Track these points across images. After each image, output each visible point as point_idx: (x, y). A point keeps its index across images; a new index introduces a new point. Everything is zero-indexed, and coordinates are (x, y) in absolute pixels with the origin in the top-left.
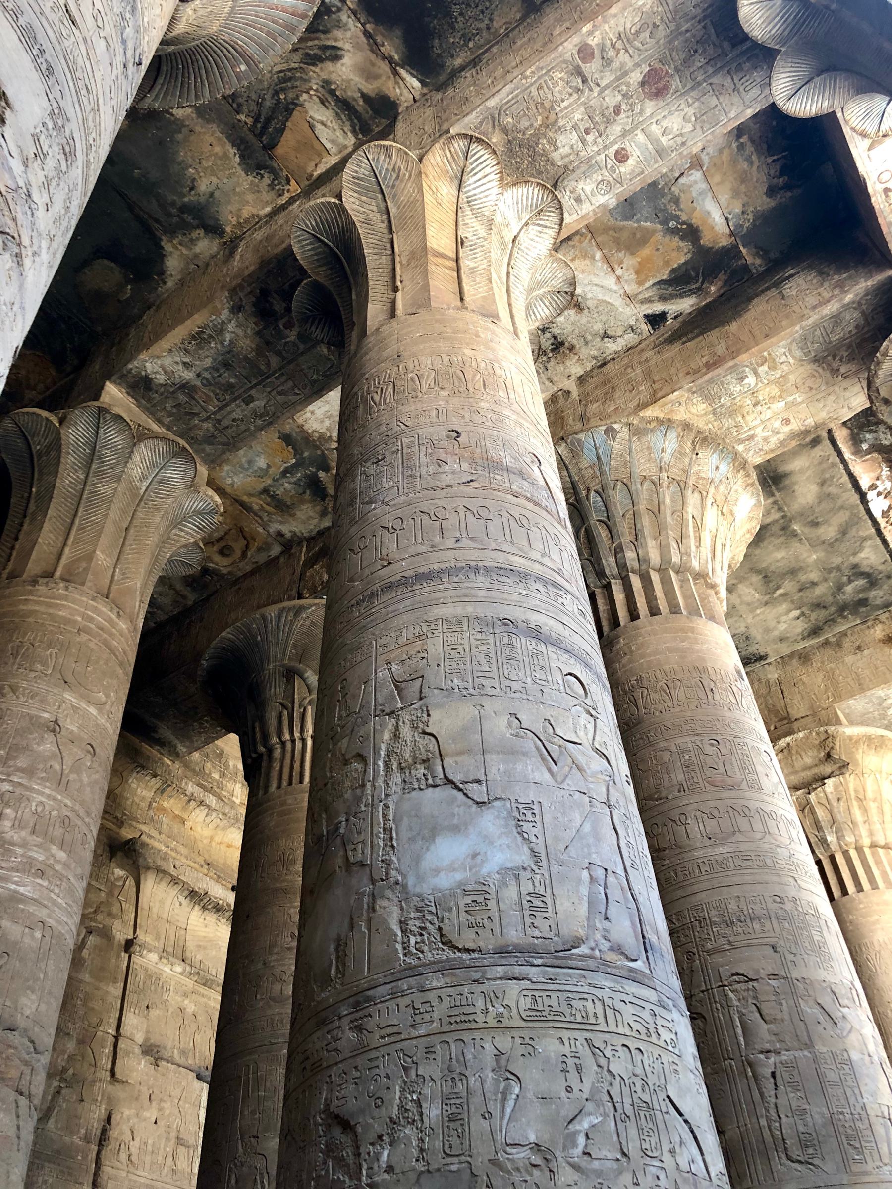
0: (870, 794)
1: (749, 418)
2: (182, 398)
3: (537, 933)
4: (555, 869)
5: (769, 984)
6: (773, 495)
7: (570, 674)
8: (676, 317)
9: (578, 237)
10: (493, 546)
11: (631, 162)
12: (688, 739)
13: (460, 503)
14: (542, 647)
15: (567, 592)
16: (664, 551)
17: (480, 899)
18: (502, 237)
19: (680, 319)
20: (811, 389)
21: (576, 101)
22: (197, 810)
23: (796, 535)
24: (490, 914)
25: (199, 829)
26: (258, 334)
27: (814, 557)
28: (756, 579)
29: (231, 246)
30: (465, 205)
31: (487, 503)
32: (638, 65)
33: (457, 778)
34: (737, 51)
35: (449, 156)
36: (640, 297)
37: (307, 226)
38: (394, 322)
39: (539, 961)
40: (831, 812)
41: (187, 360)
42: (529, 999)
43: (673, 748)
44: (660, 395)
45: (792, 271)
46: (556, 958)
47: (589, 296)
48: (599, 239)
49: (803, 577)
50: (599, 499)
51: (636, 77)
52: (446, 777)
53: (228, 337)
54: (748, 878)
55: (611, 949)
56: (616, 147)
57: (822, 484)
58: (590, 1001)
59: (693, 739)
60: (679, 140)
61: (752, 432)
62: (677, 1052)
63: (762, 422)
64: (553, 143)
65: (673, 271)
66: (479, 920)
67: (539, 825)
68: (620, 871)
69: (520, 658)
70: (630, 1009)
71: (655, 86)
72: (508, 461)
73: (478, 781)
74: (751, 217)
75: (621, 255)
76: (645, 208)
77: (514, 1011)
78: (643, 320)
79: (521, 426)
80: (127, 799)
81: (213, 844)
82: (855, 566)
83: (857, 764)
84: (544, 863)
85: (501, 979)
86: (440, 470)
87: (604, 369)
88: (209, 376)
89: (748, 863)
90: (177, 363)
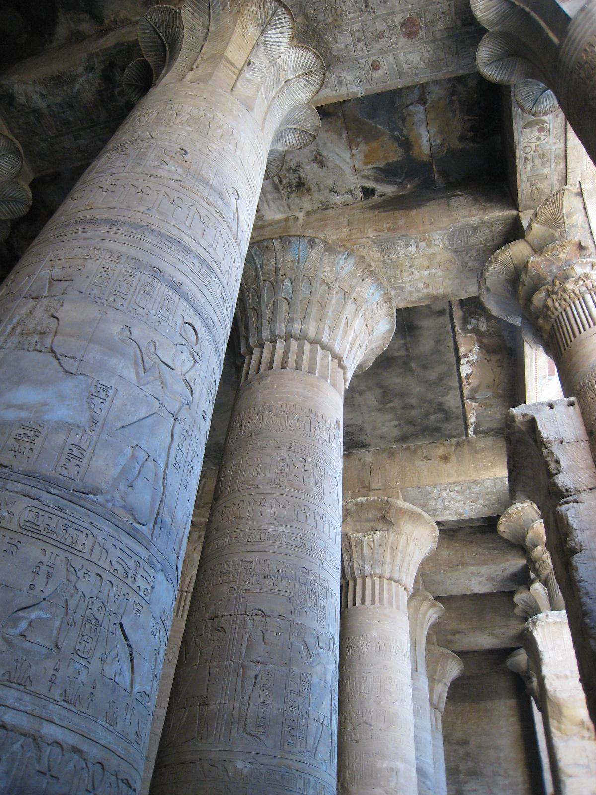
0: (400, 547)
1: (405, 274)
2: (32, 118)
3: (65, 473)
4: (104, 436)
5: (276, 621)
6: (405, 338)
7: (190, 324)
8: (381, 196)
10: (174, 222)
11: (380, 71)
12: (286, 453)
13: (163, 190)
14: (176, 297)
15: (217, 277)
16: (319, 331)
17: (31, 434)
18: (279, 75)
19: (383, 198)
20: (447, 269)
21: (358, 17)
23: (412, 371)
24: (33, 446)
26: (99, 92)
27: (418, 389)
28: (379, 391)
29: (103, 33)
30: (261, 45)
31: (184, 198)
32: (403, 12)
33: (58, 351)
35: (262, 9)
36: (363, 173)
37: (152, 21)
38: (178, 84)
39: (56, 492)
40: (373, 552)
41: (44, 93)
42: (33, 514)
43: (275, 455)
44: (354, 237)
45: (459, 193)
46: (72, 495)
47: (330, 159)
49: (407, 400)
50: (290, 284)
51: (400, 18)
52: (51, 348)
53: (78, 86)
54: (291, 552)
55: (124, 507)
56: (374, 58)
57: (438, 342)
58: (85, 535)
59: (290, 453)
60: (415, 71)
61: (404, 285)
62: (147, 598)
63: (412, 280)
64: (335, 38)
65: (388, 164)
66: (22, 447)
67: (107, 404)
68: (162, 462)
69: (155, 296)
70: (119, 553)
72: (214, 182)
73: (74, 358)
74: (445, 149)
77: (16, 518)
78: (359, 190)
79: (236, 171)
82: (440, 404)
84: (98, 429)
85: (17, 493)
86: (161, 167)
87: (326, 212)
88: (55, 110)
89: (295, 542)
90: (36, 92)
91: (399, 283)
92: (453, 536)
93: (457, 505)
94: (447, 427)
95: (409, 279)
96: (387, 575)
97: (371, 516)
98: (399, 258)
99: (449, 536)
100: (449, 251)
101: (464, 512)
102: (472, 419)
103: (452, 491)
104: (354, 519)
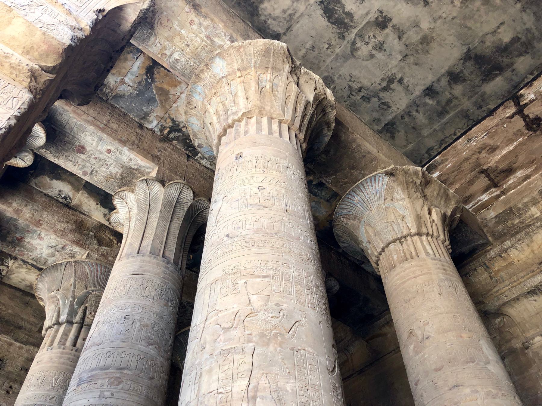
1: (197, 45)
9: (171, 116)
11: (109, 148)
20: (168, 20)
22: (510, 253)
25: (522, 256)
32: (79, 157)
34: (56, 128)
48: (168, 108)
51: (82, 156)
56: (107, 154)
60: (93, 135)
61: (205, 38)
63: (197, 36)
64: (116, 174)
71: (82, 150)
75: (171, 96)
76: (148, 95)
80: (479, 288)
81: (536, 252)
91: (206, 42)
95: (198, 38)
98: (189, 59)
100: (156, 32)
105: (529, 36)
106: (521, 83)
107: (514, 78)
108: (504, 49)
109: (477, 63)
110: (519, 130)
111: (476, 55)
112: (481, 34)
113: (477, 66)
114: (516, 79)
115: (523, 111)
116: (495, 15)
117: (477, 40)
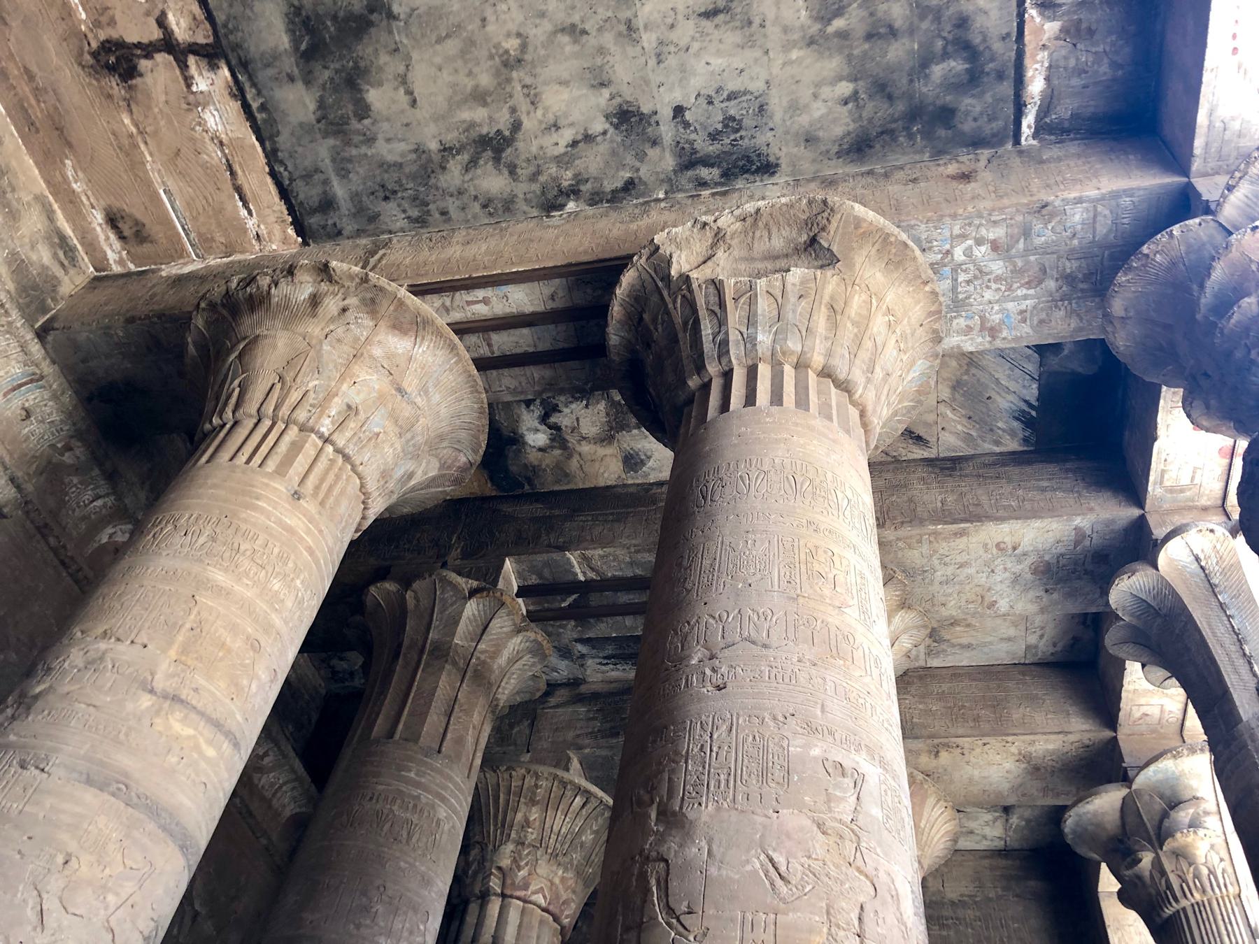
83: (851, 266)
92: (953, 469)
93: (988, 295)
94: (970, 104)
96: (818, 360)
97: (778, 243)
99: (942, 469)
101: (1002, 322)
102: (1036, 86)
103: (979, 242)
104: (736, 253)
105: (357, 139)
106: (250, 78)
107: (270, 72)
108: (353, 81)
109: (351, 17)
110: (112, 22)
111: (370, 24)
112: (415, 56)
113: (341, 14)
114: (263, 75)
115: (169, 53)
116: (440, 98)
117: (405, 41)
